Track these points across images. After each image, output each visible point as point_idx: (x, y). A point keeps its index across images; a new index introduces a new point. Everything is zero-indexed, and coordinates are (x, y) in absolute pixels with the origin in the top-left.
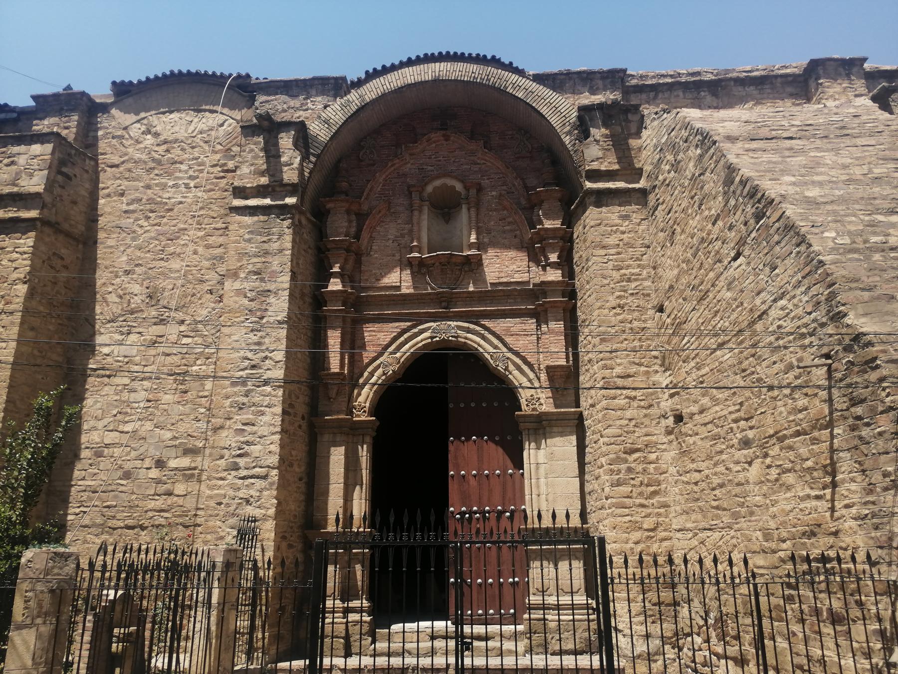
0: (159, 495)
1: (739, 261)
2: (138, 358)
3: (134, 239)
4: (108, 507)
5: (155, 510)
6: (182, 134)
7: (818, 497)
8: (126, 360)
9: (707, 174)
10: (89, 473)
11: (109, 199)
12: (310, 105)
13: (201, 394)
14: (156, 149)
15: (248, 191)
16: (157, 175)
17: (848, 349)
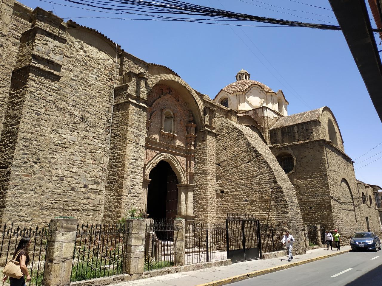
0: (84, 198)
1: (249, 163)
2: (77, 143)
3: (76, 92)
4: (65, 201)
5: (83, 204)
6: (95, 56)
7: (265, 214)
8: (73, 142)
9: (240, 140)
10: (57, 187)
11: (65, 70)
12: (140, 69)
13: (101, 162)
14: (85, 58)
15: (133, 97)
16: (85, 69)
17: (277, 188)
